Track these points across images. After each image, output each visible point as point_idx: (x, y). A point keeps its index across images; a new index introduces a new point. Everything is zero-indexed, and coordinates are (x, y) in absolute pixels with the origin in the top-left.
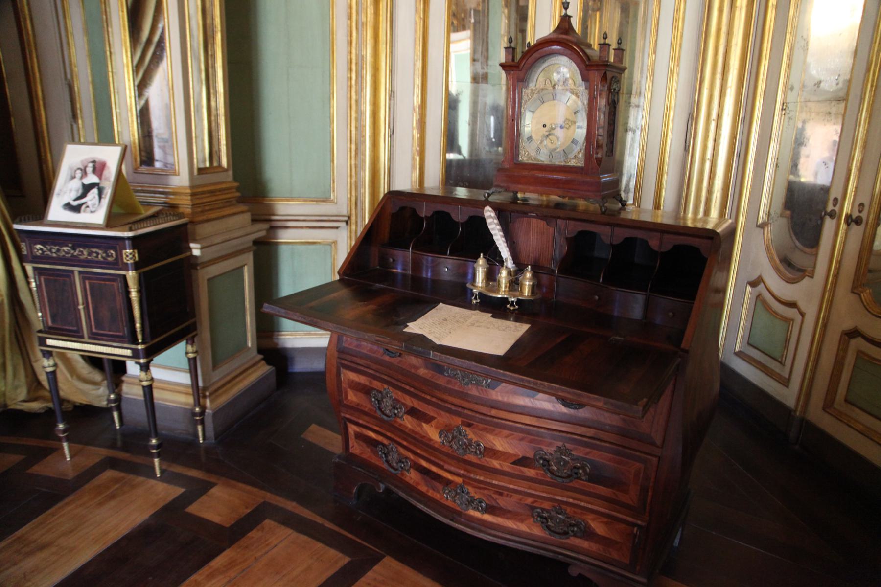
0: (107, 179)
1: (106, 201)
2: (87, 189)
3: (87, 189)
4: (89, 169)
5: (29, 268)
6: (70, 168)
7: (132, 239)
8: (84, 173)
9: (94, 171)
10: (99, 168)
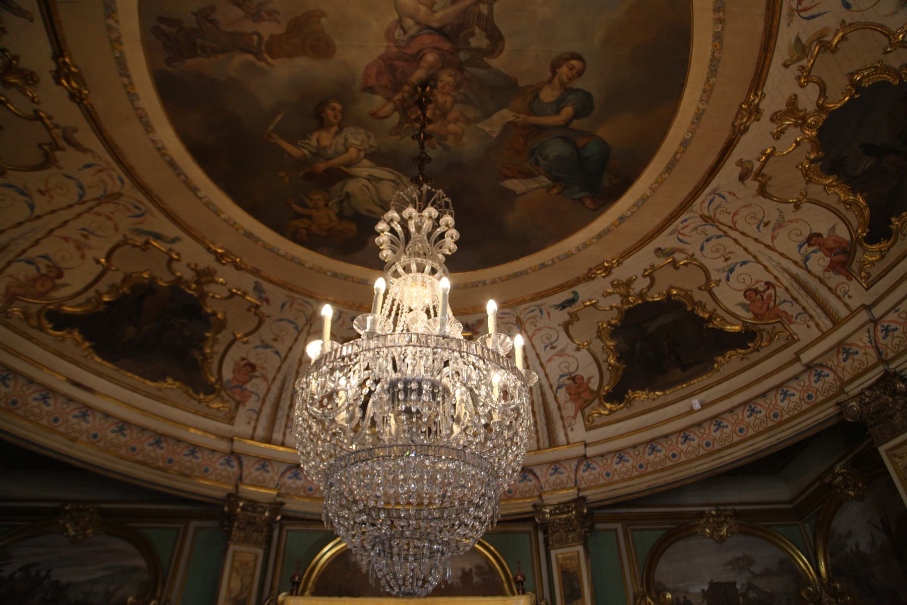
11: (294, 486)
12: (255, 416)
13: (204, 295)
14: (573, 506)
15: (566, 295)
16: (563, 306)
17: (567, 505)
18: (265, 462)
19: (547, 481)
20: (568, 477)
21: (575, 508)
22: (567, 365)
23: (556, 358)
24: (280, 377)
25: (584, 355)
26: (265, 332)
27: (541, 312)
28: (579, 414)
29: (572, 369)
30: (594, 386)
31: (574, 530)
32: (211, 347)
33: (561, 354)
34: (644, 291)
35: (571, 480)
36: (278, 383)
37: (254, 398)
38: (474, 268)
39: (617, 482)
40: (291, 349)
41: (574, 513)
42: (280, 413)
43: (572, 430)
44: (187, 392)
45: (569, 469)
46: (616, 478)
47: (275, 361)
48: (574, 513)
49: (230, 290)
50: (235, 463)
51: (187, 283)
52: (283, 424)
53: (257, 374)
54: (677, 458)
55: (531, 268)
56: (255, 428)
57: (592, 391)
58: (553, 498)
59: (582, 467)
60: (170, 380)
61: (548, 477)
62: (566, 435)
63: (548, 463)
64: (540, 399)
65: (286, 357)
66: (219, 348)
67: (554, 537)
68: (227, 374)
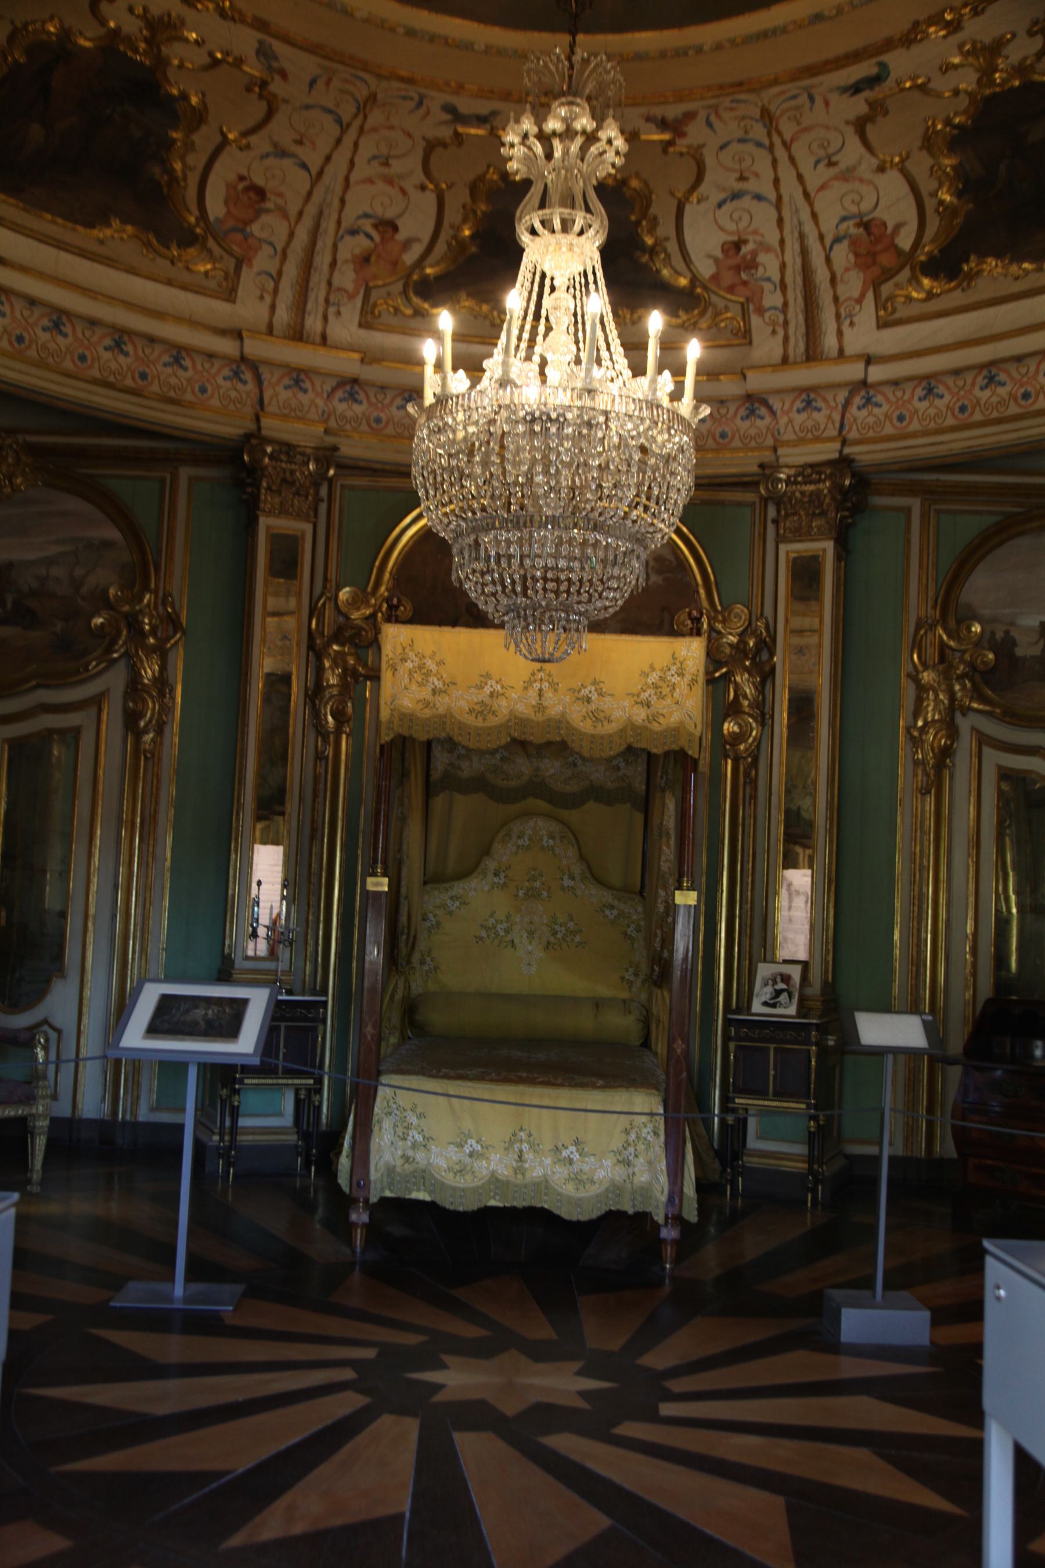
0: (794, 986)
1: (795, 1001)
2: (778, 993)
3: (778, 993)
4: (779, 979)
5: (732, 1045)
6: (763, 979)
7: (816, 1025)
8: (775, 982)
9: (783, 981)
10: (786, 979)
11: (349, 414)
12: (270, 285)
13: (162, 62)
14: (828, 472)
15: (865, 69)
16: (856, 89)
17: (817, 469)
18: (298, 376)
19: (791, 421)
20: (829, 417)
21: (829, 477)
22: (857, 198)
23: (836, 184)
24: (311, 210)
25: (893, 184)
26: (280, 129)
27: (812, 99)
28: (870, 295)
29: (866, 206)
30: (905, 241)
31: (823, 513)
32: (183, 159)
33: (847, 176)
34: (1028, 62)
35: (833, 424)
36: (307, 222)
37: (267, 250)
38: (680, 23)
39: (914, 435)
40: (328, 159)
41: (828, 484)
42: (314, 278)
43: (852, 324)
44: (148, 245)
45: (833, 404)
46: (915, 426)
47: (301, 181)
48: (828, 484)
49: (211, 54)
50: (248, 376)
51: (129, 40)
52: (321, 300)
53: (269, 205)
54: (1030, 401)
55: (795, 22)
56: (273, 308)
57: (899, 252)
58: (795, 456)
59: (857, 401)
60: (116, 223)
61: (794, 415)
62: (840, 333)
63: (793, 390)
64: (799, 261)
65: (320, 173)
66: (197, 160)
67: (788, 524)
68: (215, 208)
